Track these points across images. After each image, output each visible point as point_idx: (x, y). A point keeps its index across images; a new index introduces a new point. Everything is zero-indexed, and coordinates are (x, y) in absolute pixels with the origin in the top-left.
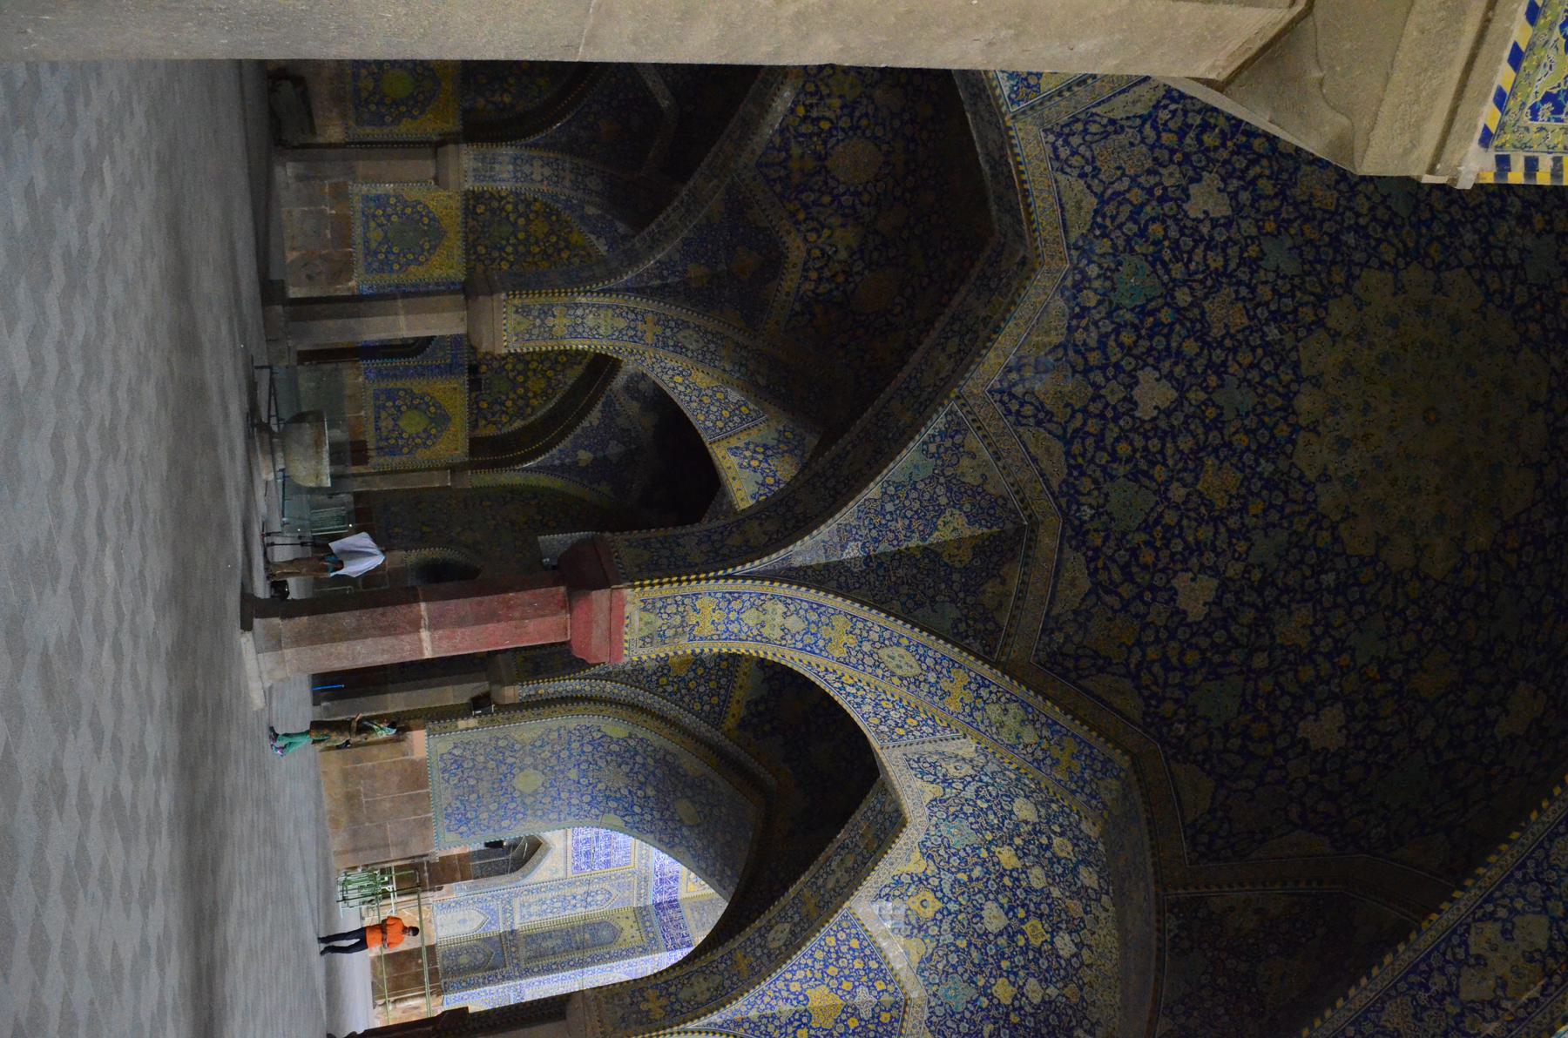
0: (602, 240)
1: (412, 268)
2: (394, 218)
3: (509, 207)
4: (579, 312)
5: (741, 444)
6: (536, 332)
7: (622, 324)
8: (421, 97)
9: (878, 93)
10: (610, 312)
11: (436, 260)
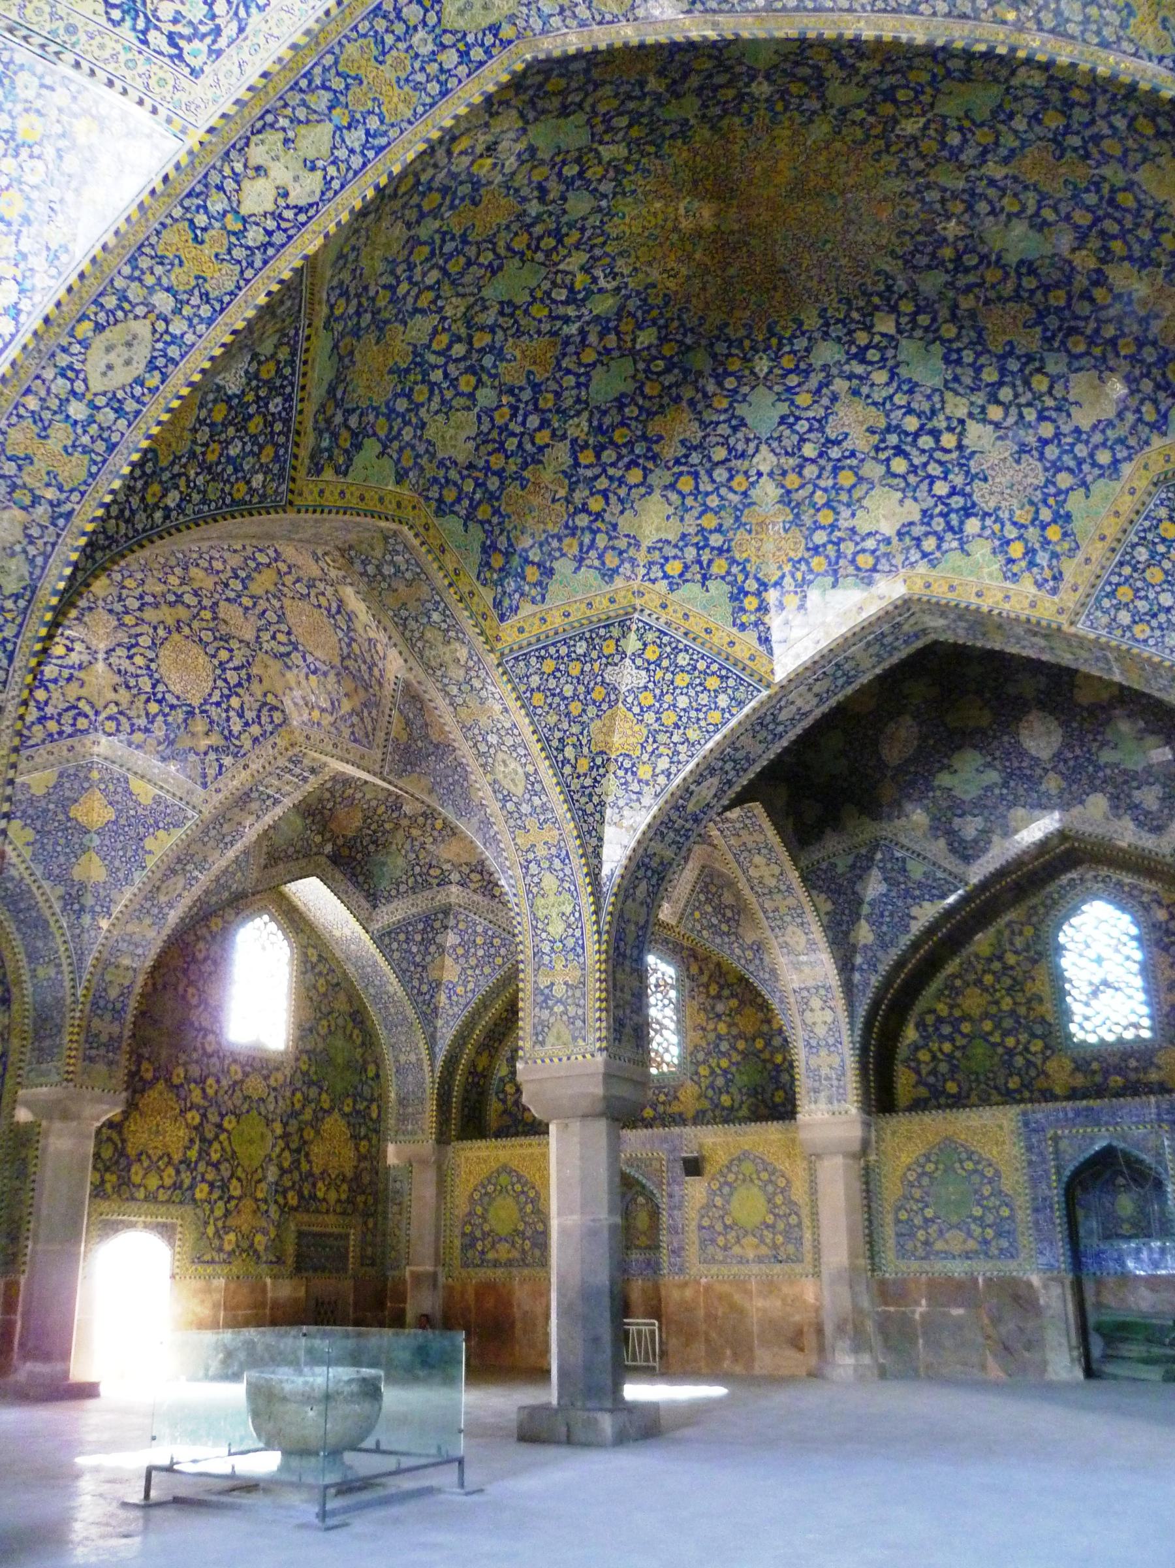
0: (915, 911)
1: (1007, 1185)
2: (929, 1213)
3: (947, 1047)
4: (546, 947)
5: (750, 637)
6: (572, 1011)
7: (549, 882)
8: (765, 1176)
9: (249, 636)
10: (540, 901)
11: (992, 1152)
